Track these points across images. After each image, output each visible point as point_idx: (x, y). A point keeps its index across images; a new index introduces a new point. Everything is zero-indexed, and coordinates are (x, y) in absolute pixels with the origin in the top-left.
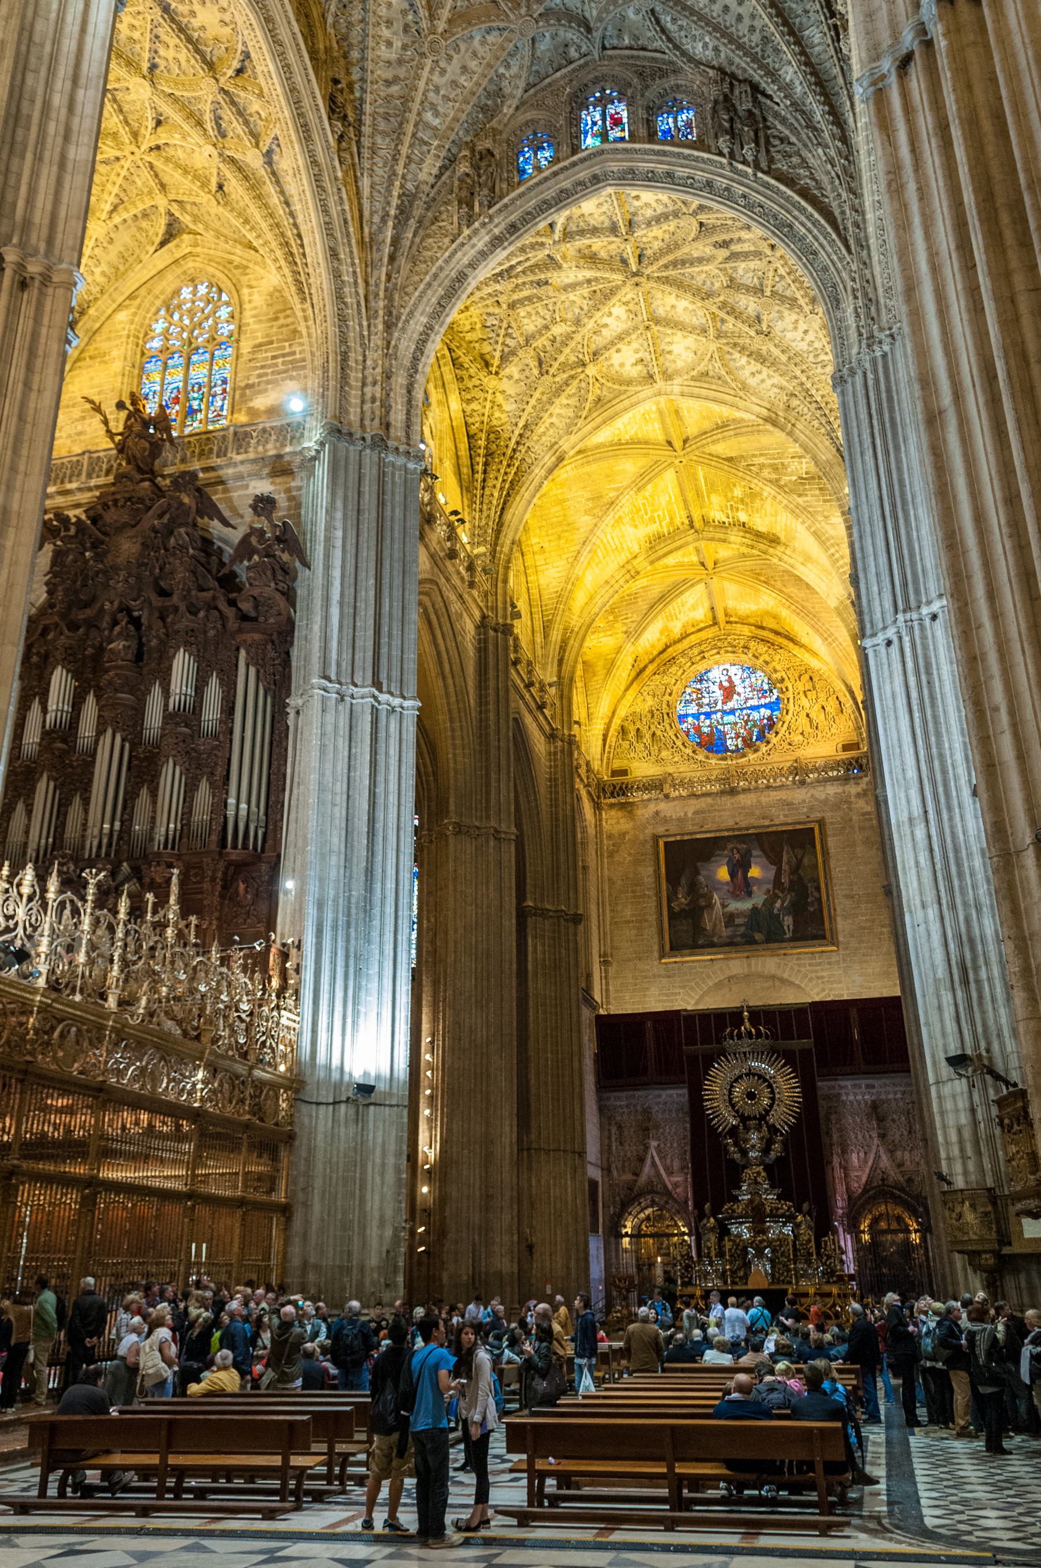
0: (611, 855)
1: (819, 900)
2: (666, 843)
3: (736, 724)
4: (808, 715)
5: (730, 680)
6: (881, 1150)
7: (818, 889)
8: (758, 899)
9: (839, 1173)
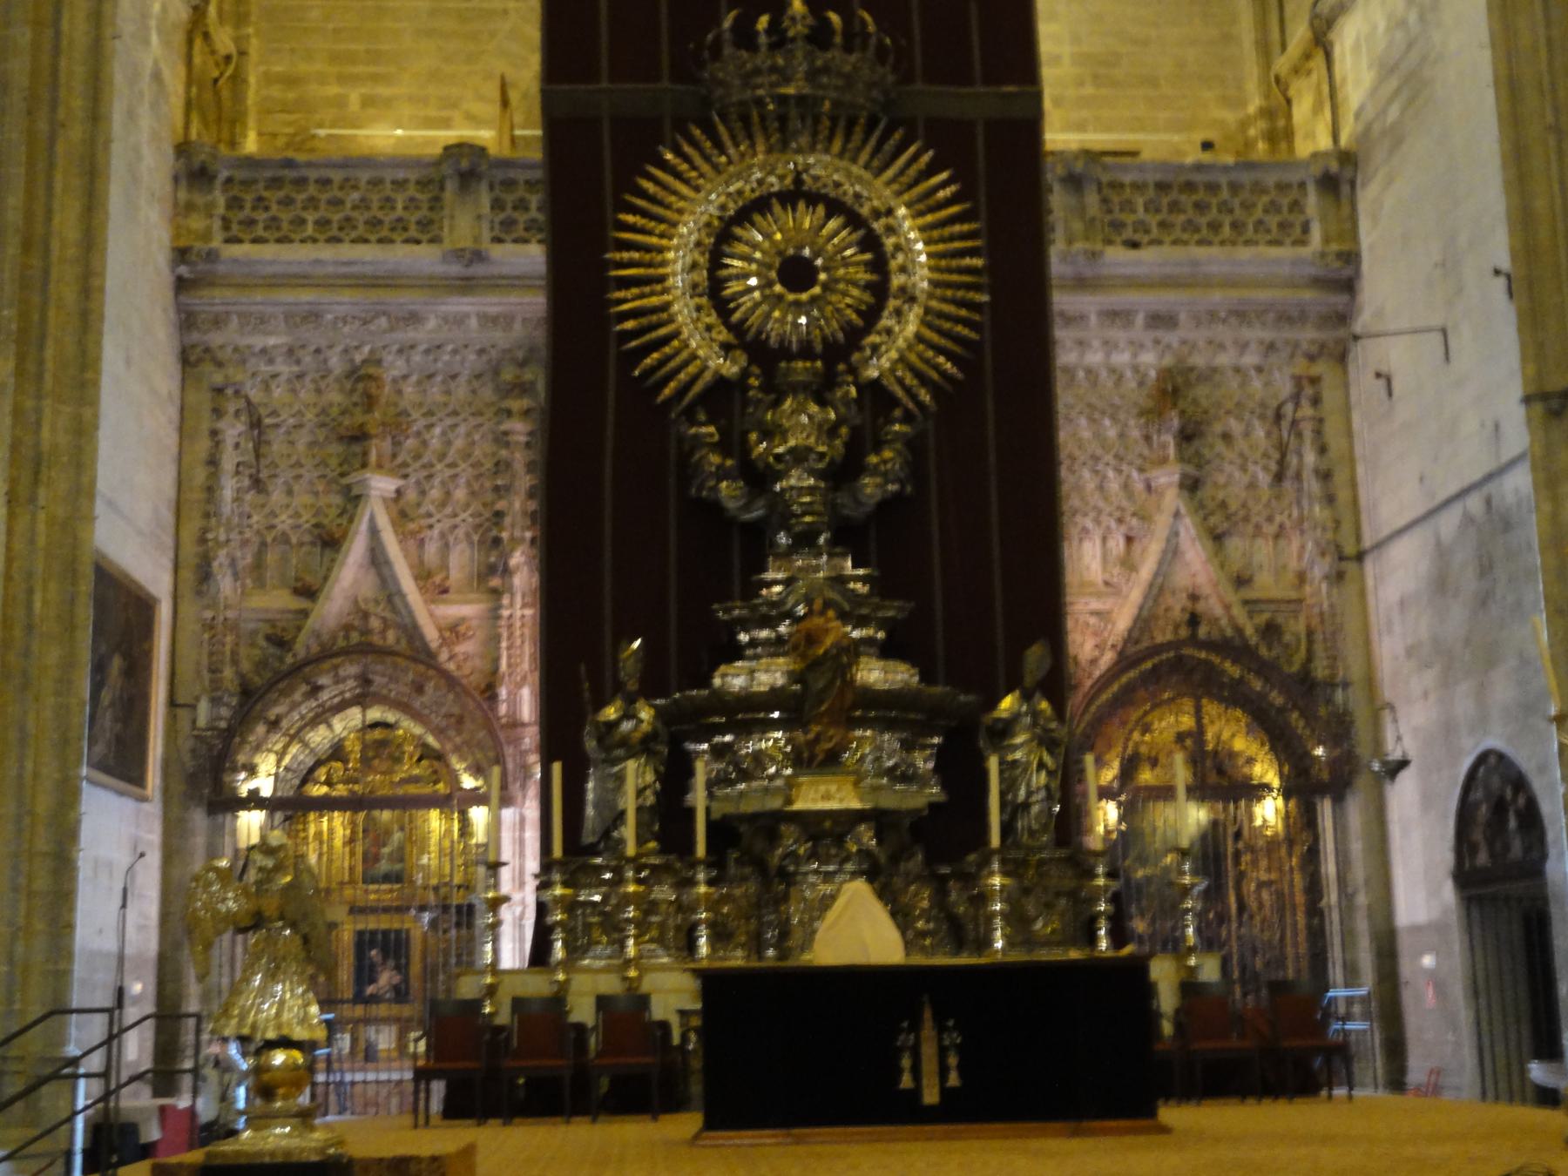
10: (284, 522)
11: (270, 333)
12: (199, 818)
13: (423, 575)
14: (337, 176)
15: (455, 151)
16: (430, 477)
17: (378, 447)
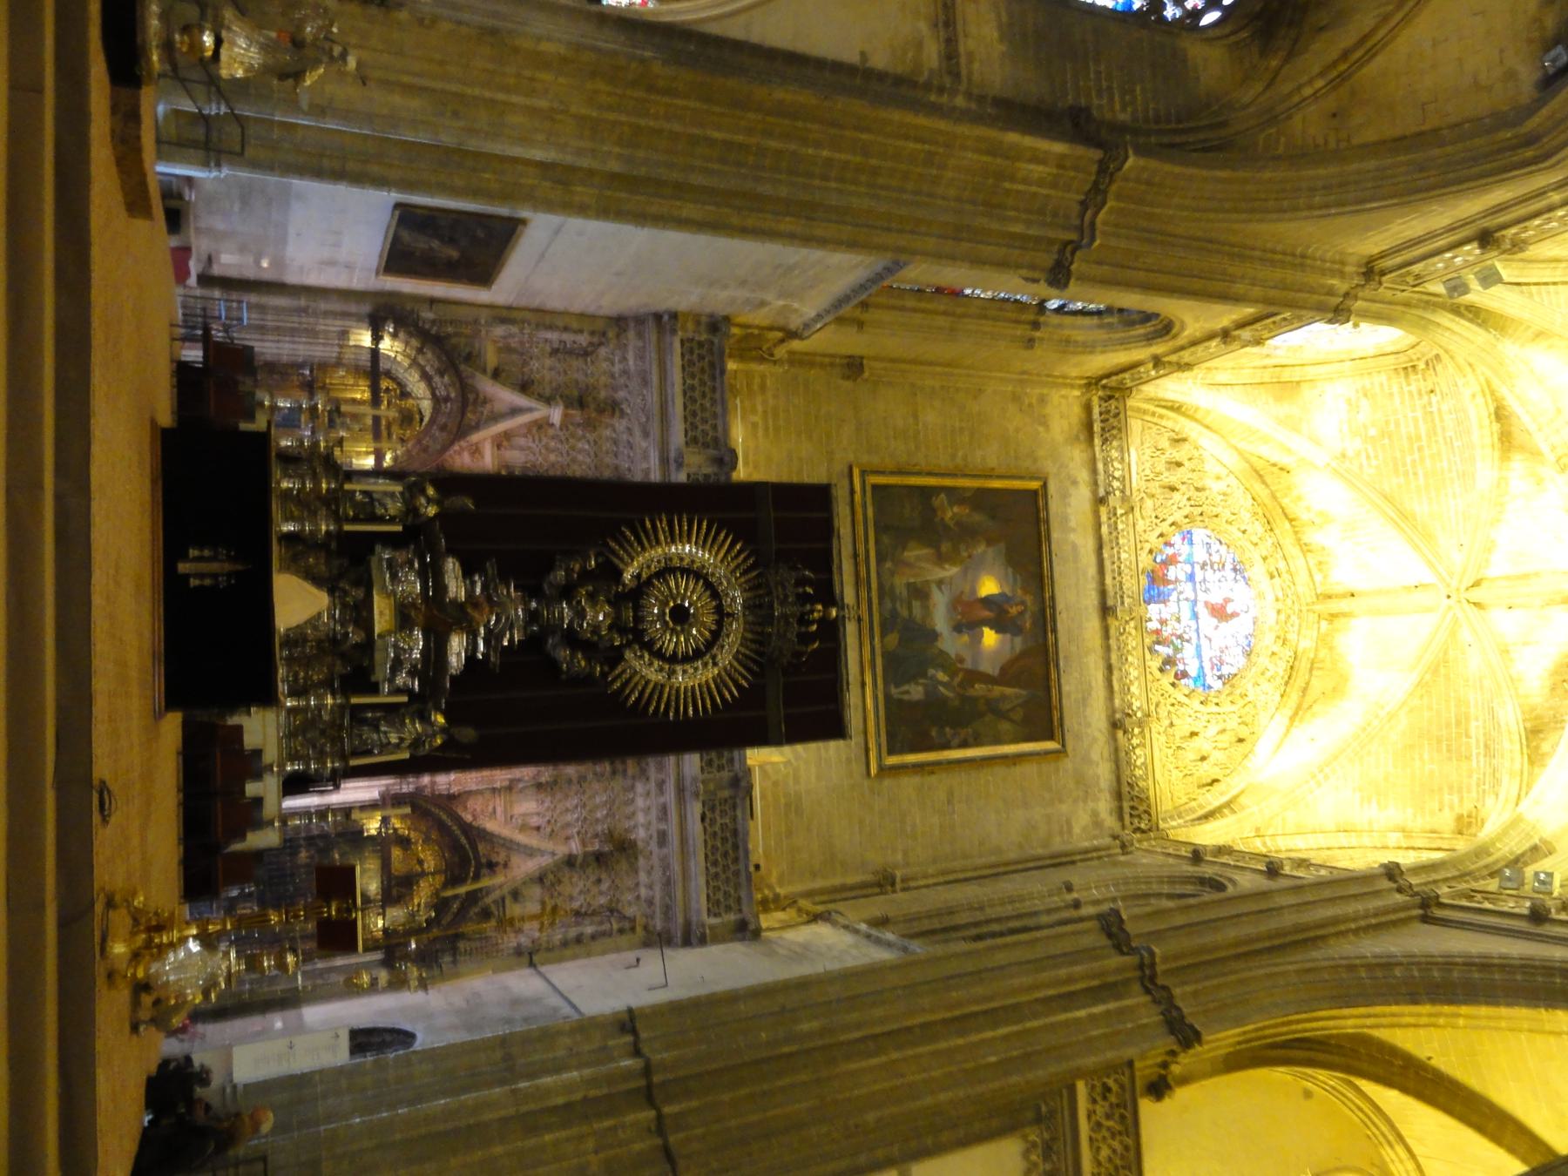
0: (1016, 398)
1: (946, 746)
2: (1035, 492)
3: (1178, 620)
4: (1193, 734)
5: (1234, 615)
6: (545, 861)
7: (964, 744)
8: (951, 643)
9: (501, 776)
10: (535, 365)
11: (635, 360)
12: (366, 308)
13: (507, 435)
14: (718, 396)
15: (733, 453)
16: (561, 442)
17: (576, 414)
